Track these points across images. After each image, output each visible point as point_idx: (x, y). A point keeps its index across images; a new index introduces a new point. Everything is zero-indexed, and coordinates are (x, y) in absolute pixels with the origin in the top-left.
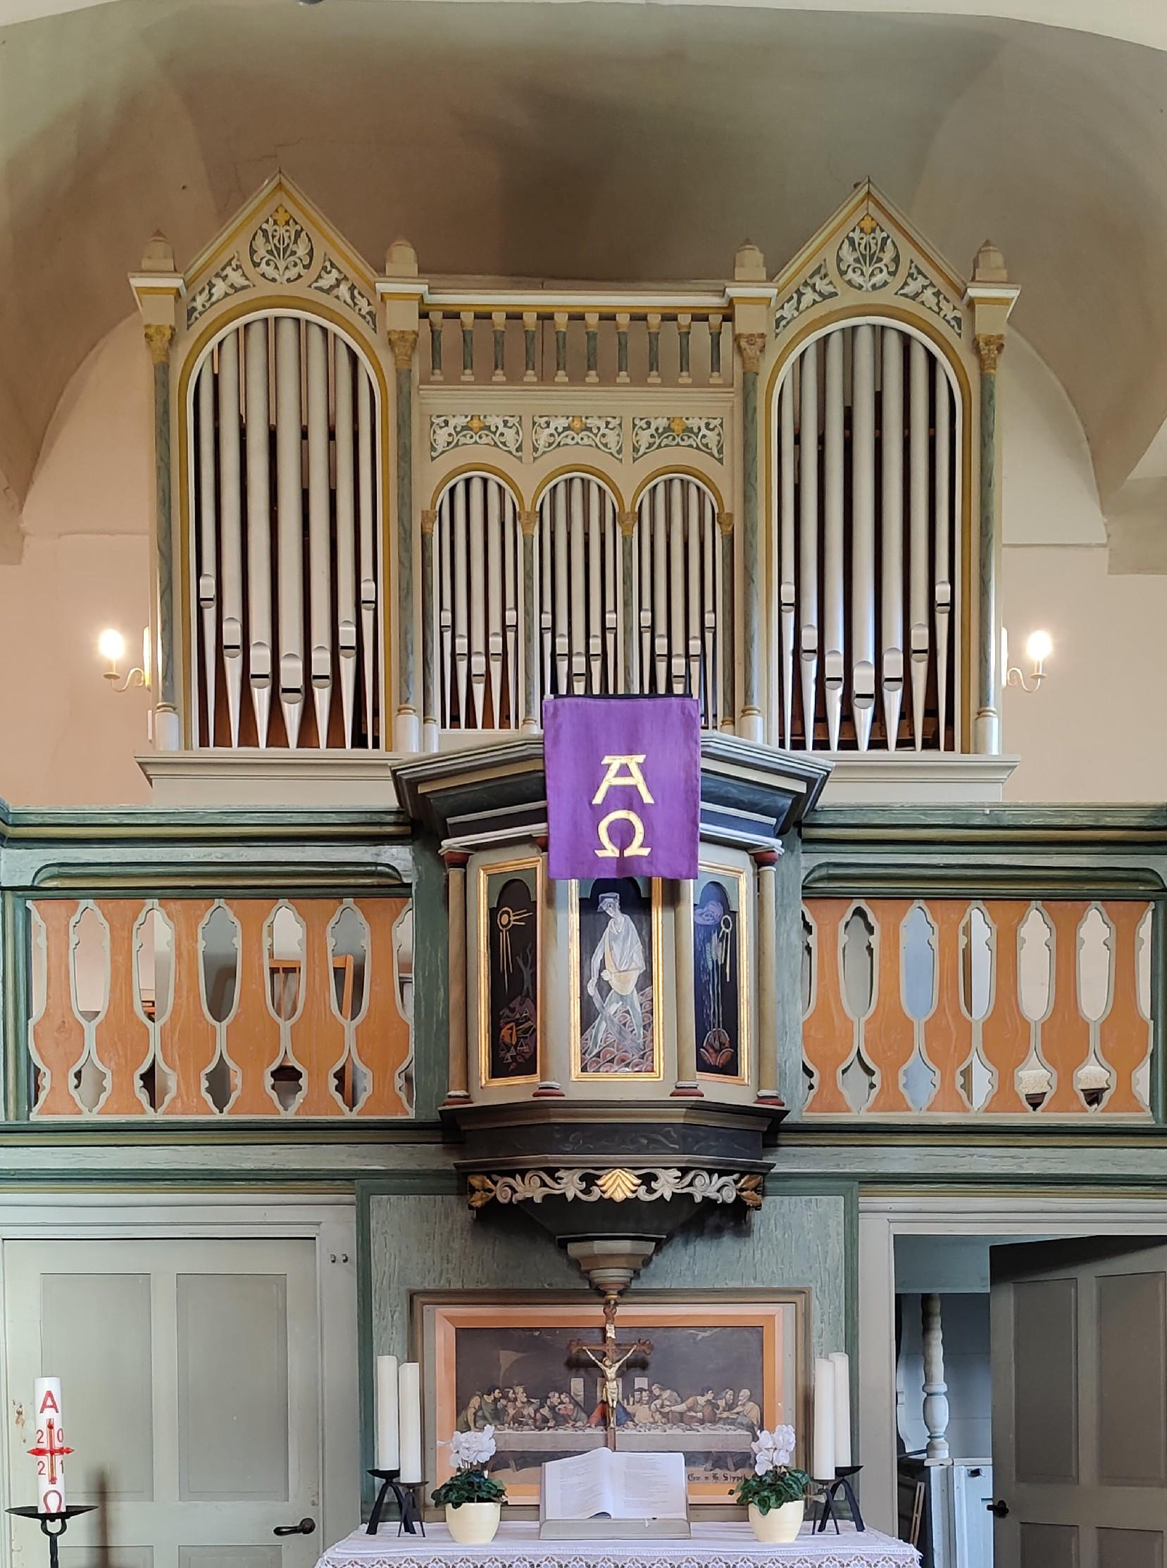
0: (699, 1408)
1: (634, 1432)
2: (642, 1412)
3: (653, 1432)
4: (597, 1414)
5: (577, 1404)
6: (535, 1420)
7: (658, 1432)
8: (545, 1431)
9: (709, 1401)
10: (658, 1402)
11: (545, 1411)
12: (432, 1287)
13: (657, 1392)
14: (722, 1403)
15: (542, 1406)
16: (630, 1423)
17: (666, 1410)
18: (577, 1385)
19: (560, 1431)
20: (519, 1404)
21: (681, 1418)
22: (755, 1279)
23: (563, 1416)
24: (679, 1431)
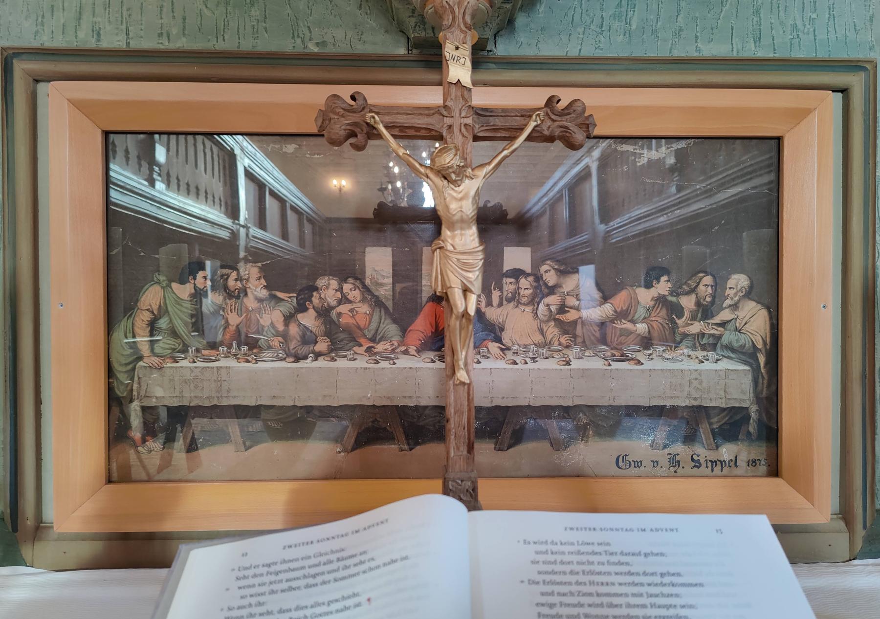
0: (641, 312)
1: (501, 364)
2: (519, 323)
3: (542, 364)
4: (421, 326)
5: (378, 303)
6: (285, 336)
7: (552, 364)
8: (308, 363)
9: (660, 300)
10: (553, 300)
11: (309, 319)
12: (59, 42)
13: (551, 278)
14: (688, 302)
15: (302, 308)
16: (494, 347)
17: (571, 316)
18: (379, 261)
19: (341, 363)
20: (250, 302)
21: (603, 336)
22: (758, 40)
23: (348, 330)
24: (597, 364)
